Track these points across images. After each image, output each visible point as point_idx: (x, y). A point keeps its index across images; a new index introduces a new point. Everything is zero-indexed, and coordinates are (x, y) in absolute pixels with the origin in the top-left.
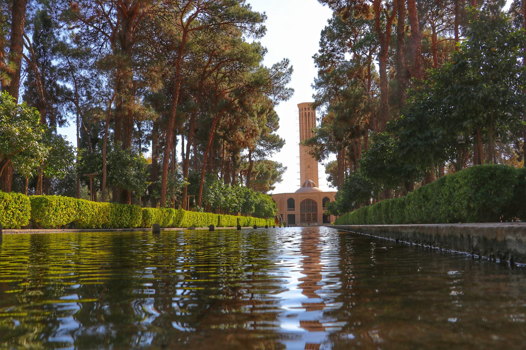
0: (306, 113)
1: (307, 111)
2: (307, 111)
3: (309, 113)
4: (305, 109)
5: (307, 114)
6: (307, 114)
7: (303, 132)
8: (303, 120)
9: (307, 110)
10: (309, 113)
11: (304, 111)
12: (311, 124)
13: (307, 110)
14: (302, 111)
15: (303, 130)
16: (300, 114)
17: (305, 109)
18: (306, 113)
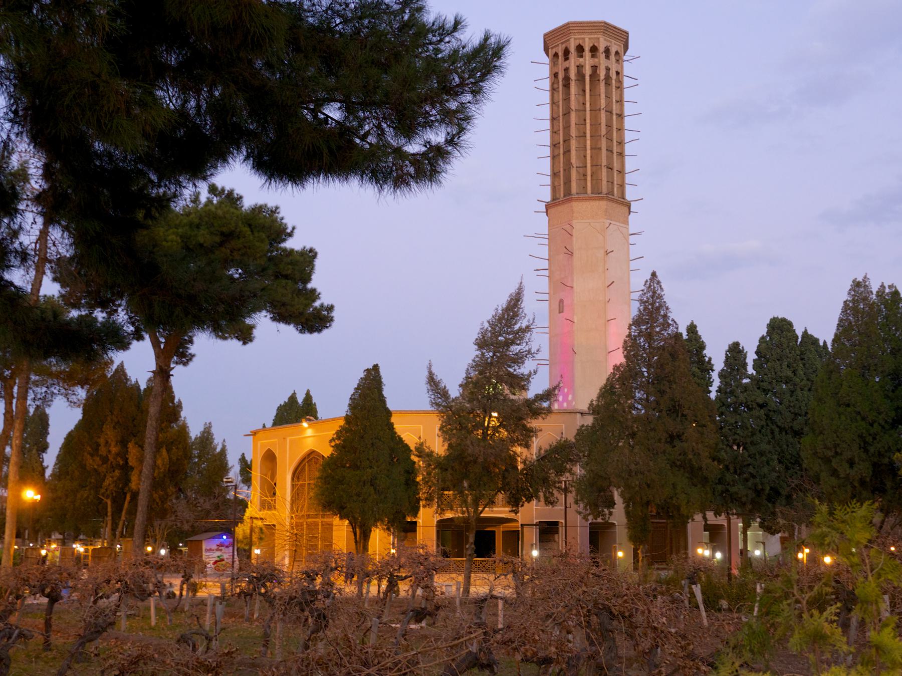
0: (580, 68)
1: (587, 61)
2: (587, 61)
3: (595, 68)
4: (580, 49)
5: (588, 71)
6: (588, 71)
7: (567, 152)
8: (567, 99)
9: (587, 53)
10: (595, 68)
11: (573, 61)
12: (603, 115)
13: (587, 53)
14: (566, 58)
15: (567, 141)
16: (556, 75)
17: (580, 49)
18: (580, 68)
